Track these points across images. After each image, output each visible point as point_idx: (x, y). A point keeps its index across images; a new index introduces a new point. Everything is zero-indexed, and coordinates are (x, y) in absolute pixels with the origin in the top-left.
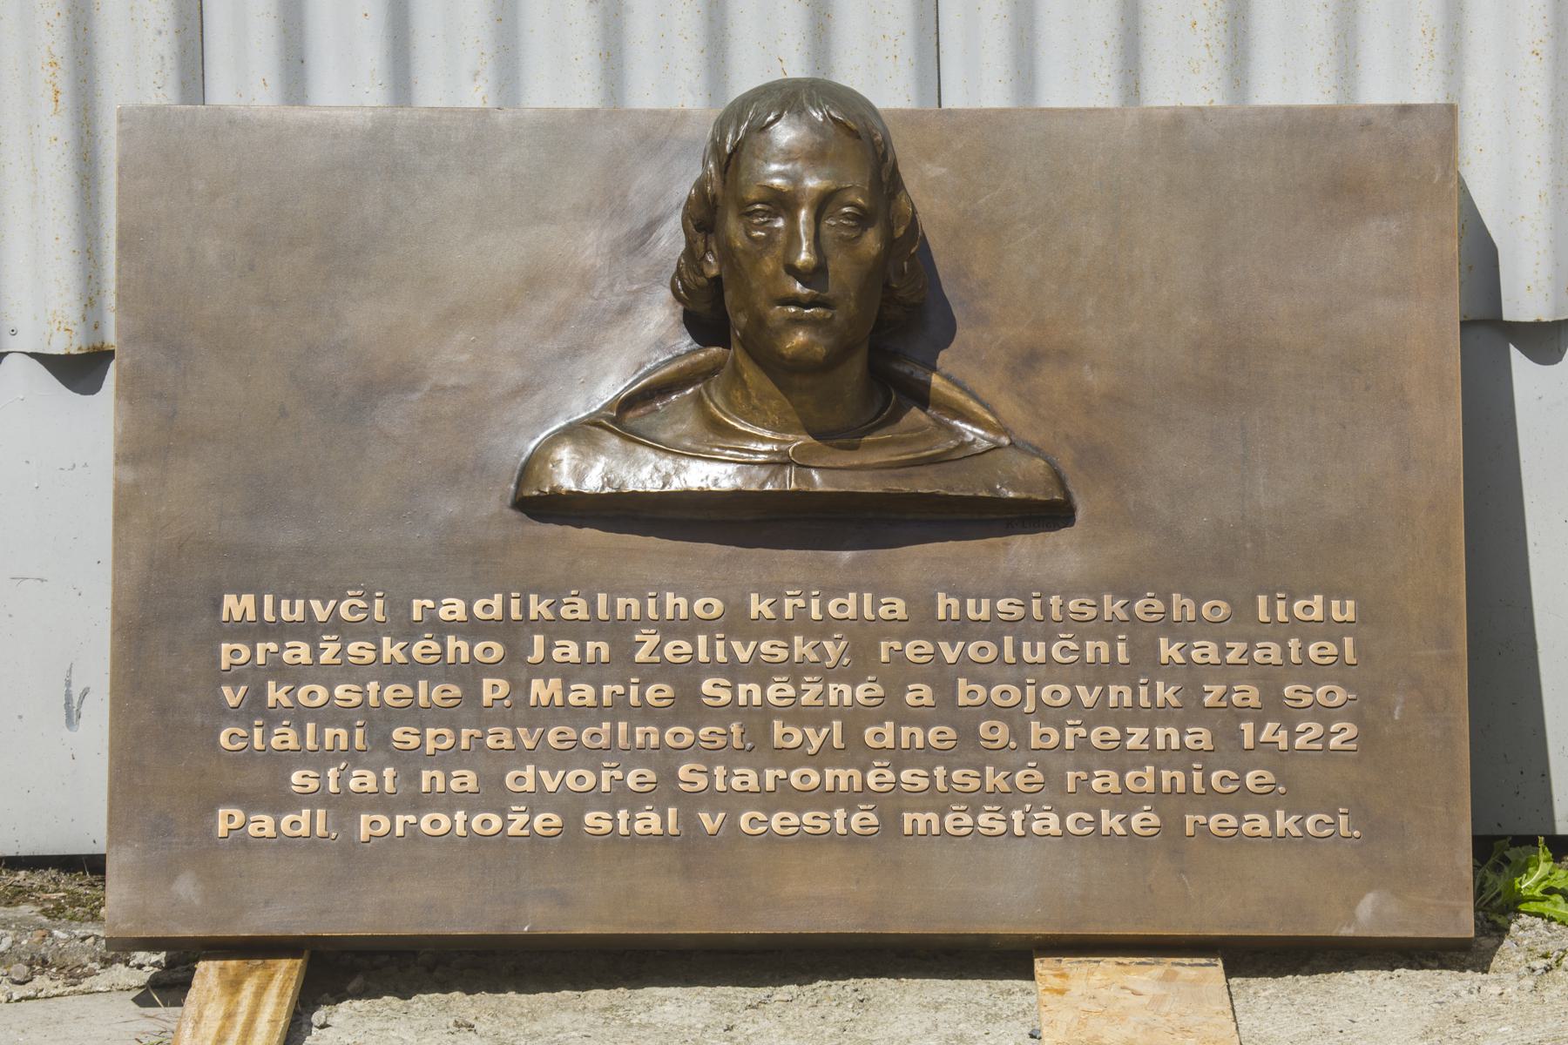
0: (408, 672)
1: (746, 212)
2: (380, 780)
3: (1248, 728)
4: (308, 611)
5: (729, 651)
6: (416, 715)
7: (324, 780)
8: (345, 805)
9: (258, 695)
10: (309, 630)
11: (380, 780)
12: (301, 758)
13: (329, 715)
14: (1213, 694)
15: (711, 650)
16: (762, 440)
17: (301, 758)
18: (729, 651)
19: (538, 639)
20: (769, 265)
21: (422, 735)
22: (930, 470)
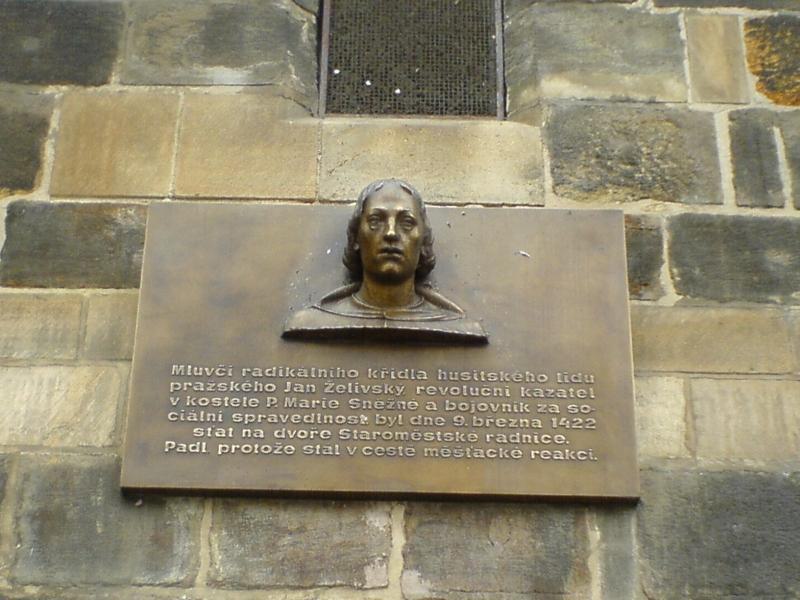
0: (240, 393)
1: (370, 220)
2: (227, 433)
3: (554, 420)
4: (204, 371)
5: (360, 389)
6: (239, 408)
7: (206, 432)
8: (213, 441)
9: (182, 401)
10: (204, 378)
11: (227, 433)
12: (198, 423)
13: (209, 408)
14: (542, 406)
15: (353, 389)
16: (372, 309)
17: (198, 423)
18: (360, 389)
19: (289, 383)
20: (378, 237)
21: (243, 417)
22: (436, 323)
